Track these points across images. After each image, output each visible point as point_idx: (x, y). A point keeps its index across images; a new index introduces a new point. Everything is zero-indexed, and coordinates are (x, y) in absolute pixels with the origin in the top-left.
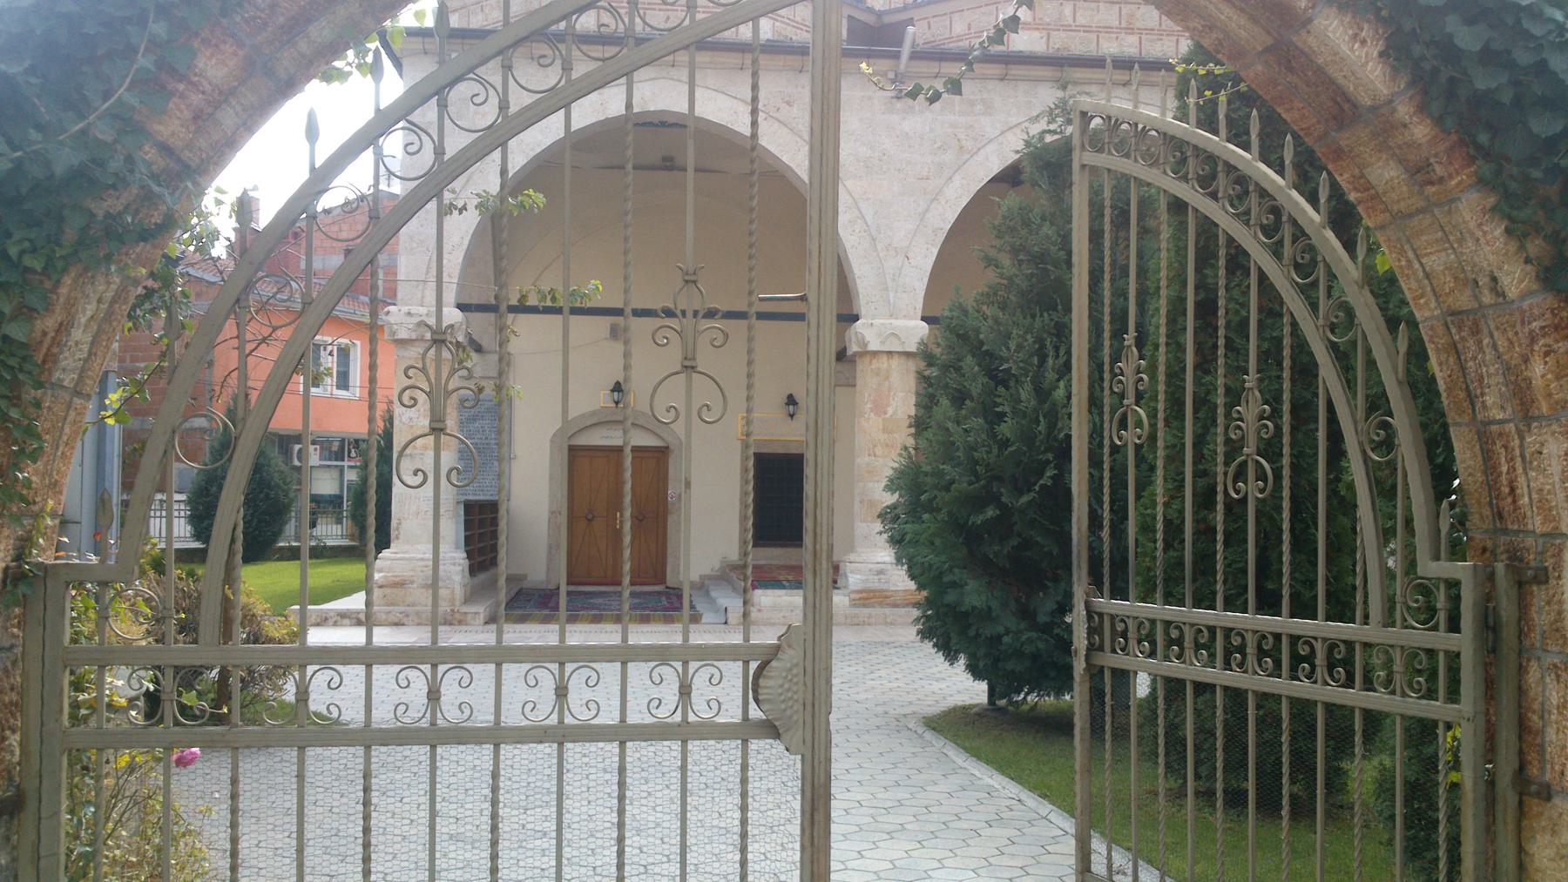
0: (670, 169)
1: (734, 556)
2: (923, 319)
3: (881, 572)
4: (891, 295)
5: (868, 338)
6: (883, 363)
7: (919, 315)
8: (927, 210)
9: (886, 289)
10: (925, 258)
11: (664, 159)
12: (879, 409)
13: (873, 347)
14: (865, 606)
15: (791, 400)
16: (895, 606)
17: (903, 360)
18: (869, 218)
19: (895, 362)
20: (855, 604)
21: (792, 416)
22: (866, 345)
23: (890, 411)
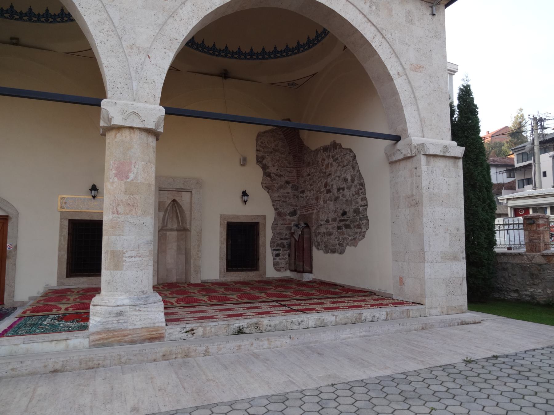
0: (17, 44)
1: (53, 282)
2: (160, 105)
3: (120, 314)
4: (135, 83)
5: (111, 115)
6: (126, 135)
7: (158, 101)
8: (165, 23)
9: (131, 79)
10: (164, 59)
11: (11, 38)
12: (122, 174)
13: (117, 121)
14: (104, 345)
15: (94, 188)
16: (133, 342)
17: (144, 135)
18: (116, 21)
19: (137, 137)
20: (94, 345)
21: (94, 197)
22: (110, 120)
23: (132, 176)
